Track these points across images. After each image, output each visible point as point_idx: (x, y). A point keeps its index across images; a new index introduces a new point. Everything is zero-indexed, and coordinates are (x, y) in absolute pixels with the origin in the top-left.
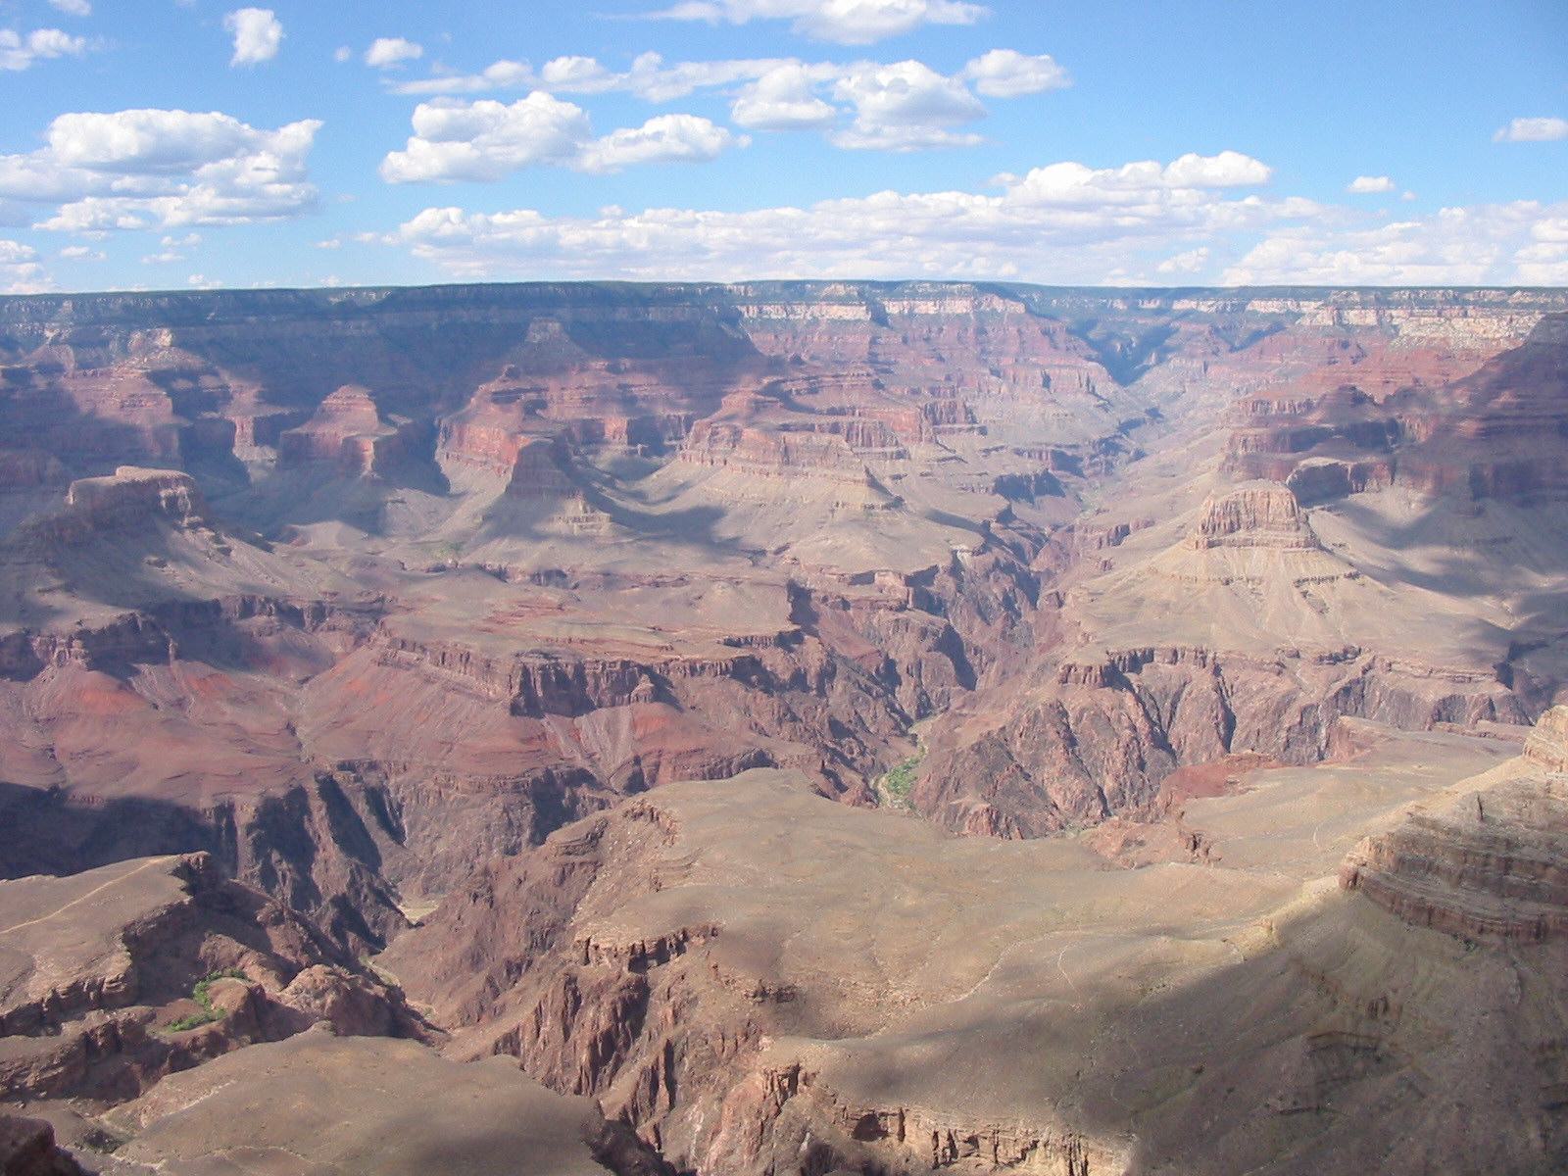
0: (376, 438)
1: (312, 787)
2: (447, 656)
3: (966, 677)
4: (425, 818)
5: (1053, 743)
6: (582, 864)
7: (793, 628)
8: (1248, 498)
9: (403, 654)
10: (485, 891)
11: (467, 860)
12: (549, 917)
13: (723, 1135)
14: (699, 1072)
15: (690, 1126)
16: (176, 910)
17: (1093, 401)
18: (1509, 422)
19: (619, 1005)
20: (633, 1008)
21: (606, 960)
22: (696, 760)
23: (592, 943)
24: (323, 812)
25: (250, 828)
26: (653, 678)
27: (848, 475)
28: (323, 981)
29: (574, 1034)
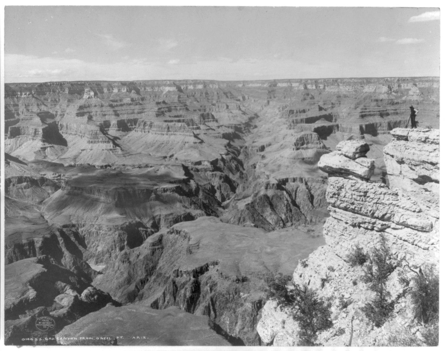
0: (42, 128)
1: (58, 233)
2: (92, 191)
3: (233, 189)
4: (92, 240)
5: (266, 206)
6: (158, 249)
7: (185, 177)
8: (306, 136)
9: (76, 191)
10: (126, 260)
11: (109, 252)
12: (151, 265)
13: (240, 322)
14: (222, 305)
15: (224, 322)
16: (43, 273)
17: (240, 112)
18: (367, 113)
19: (193, 288)
20: (197, 288)
21: (184, 275)
22: (171, 217)
23: (180, 270)
24: (62, 241)
25: (40, 248)
26: (155, 194)
27: (188, 134)
28: (93, 292)
29: (177, 299)
